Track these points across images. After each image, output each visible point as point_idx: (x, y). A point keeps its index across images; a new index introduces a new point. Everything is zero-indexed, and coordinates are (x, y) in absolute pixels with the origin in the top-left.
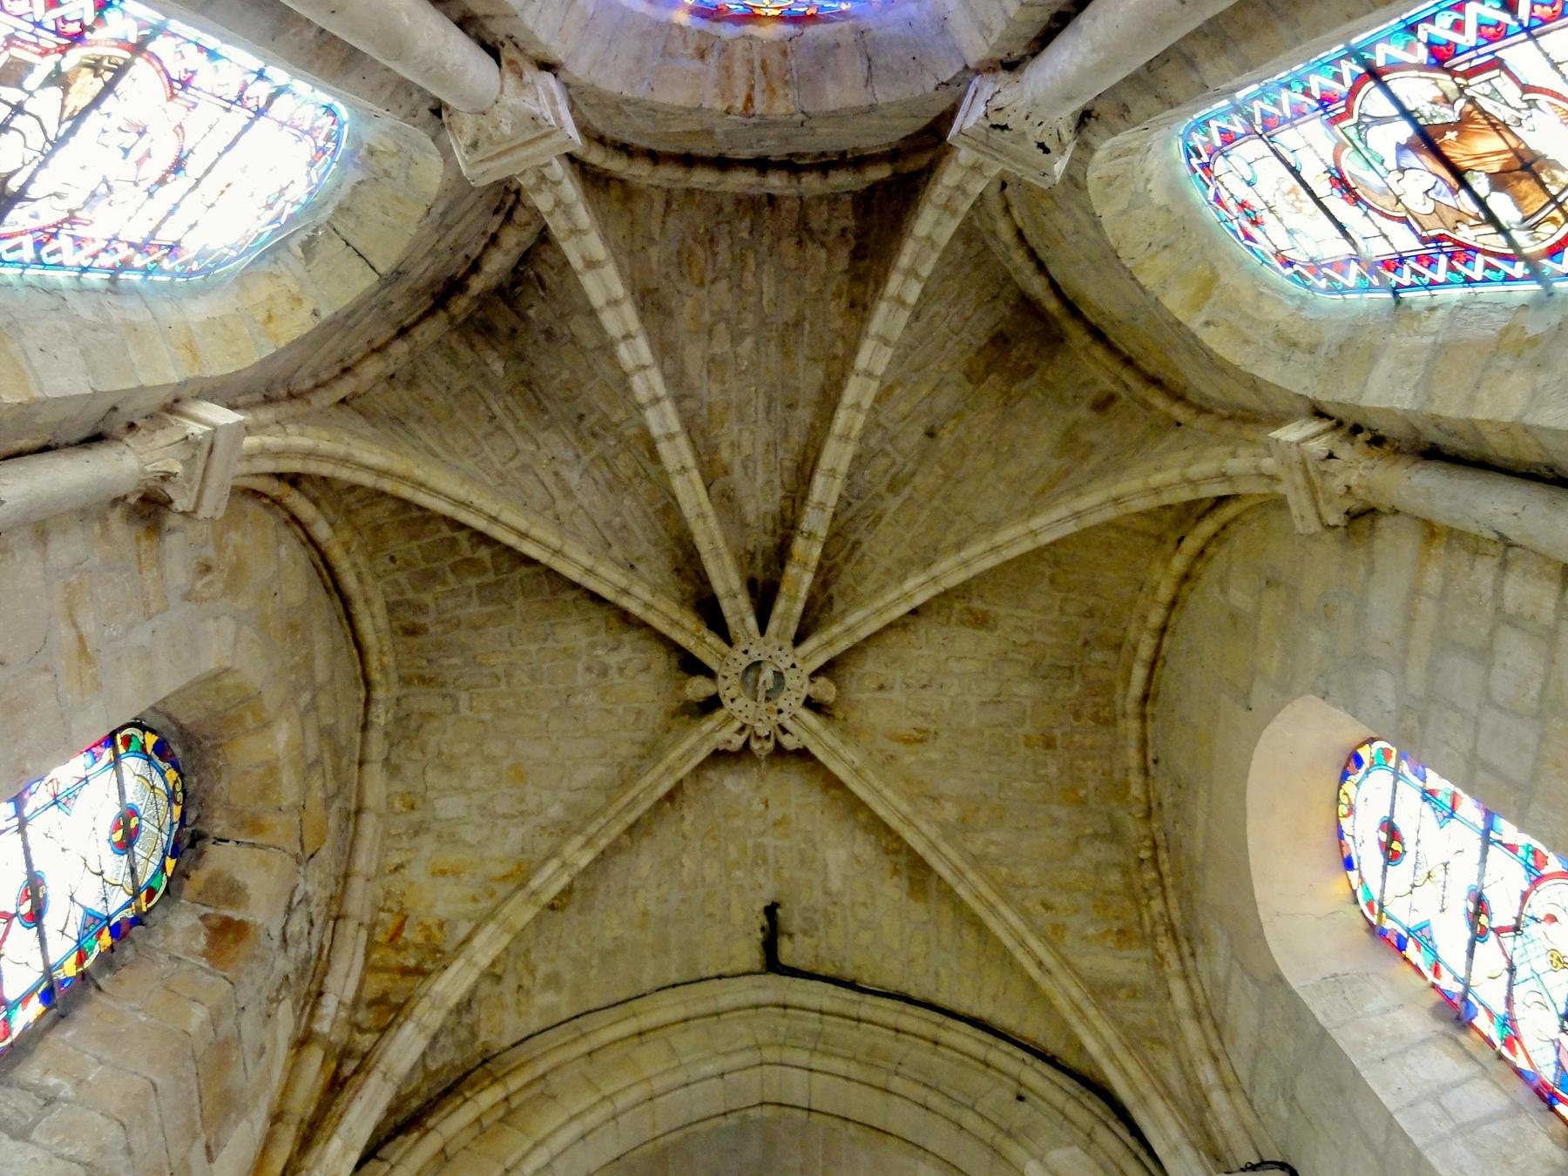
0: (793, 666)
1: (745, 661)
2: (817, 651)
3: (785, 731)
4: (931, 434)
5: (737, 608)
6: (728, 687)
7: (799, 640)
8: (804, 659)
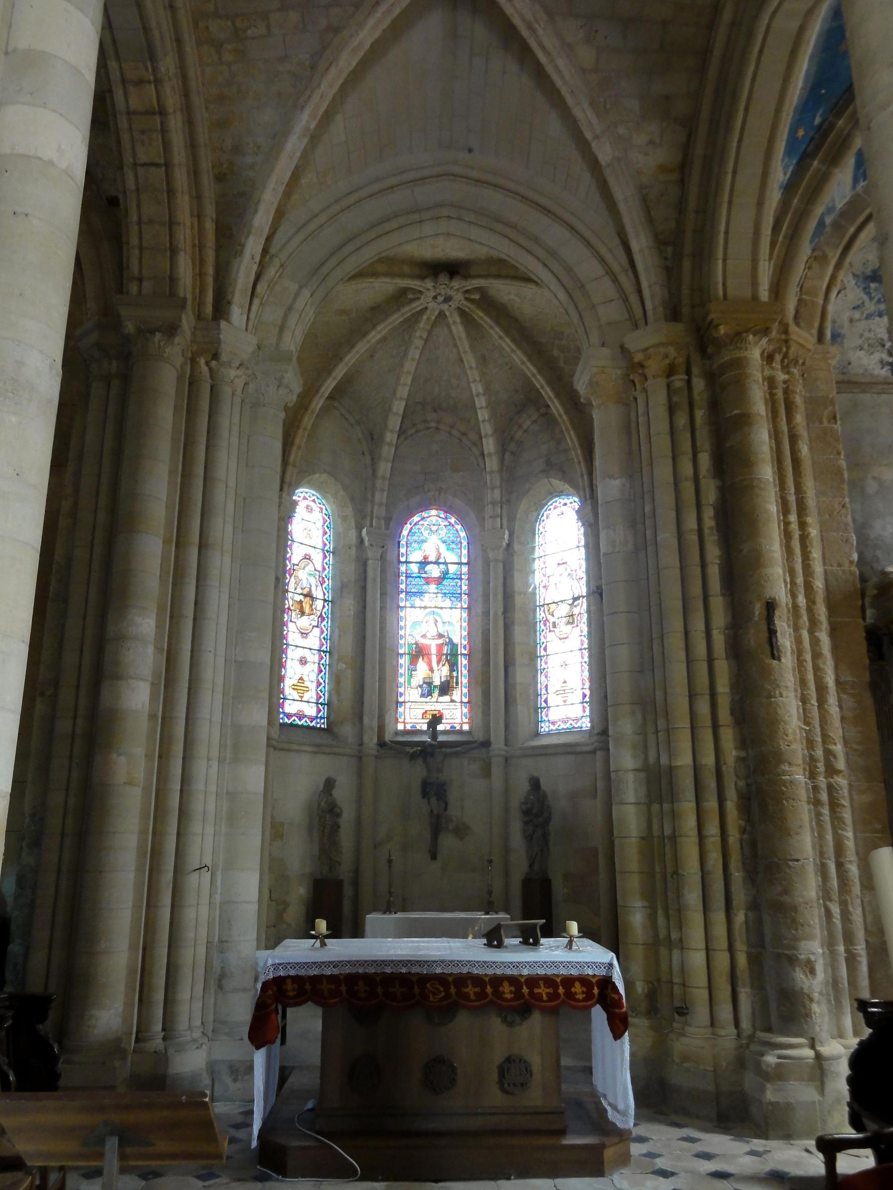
0: (428, 303)
1: (450, 303)
2: (417, 306)
3: (434, 287)
4: (372, 356)
5: (455, 318)
6: (458, 297)
7: (426, 308)
8: (422, 304)
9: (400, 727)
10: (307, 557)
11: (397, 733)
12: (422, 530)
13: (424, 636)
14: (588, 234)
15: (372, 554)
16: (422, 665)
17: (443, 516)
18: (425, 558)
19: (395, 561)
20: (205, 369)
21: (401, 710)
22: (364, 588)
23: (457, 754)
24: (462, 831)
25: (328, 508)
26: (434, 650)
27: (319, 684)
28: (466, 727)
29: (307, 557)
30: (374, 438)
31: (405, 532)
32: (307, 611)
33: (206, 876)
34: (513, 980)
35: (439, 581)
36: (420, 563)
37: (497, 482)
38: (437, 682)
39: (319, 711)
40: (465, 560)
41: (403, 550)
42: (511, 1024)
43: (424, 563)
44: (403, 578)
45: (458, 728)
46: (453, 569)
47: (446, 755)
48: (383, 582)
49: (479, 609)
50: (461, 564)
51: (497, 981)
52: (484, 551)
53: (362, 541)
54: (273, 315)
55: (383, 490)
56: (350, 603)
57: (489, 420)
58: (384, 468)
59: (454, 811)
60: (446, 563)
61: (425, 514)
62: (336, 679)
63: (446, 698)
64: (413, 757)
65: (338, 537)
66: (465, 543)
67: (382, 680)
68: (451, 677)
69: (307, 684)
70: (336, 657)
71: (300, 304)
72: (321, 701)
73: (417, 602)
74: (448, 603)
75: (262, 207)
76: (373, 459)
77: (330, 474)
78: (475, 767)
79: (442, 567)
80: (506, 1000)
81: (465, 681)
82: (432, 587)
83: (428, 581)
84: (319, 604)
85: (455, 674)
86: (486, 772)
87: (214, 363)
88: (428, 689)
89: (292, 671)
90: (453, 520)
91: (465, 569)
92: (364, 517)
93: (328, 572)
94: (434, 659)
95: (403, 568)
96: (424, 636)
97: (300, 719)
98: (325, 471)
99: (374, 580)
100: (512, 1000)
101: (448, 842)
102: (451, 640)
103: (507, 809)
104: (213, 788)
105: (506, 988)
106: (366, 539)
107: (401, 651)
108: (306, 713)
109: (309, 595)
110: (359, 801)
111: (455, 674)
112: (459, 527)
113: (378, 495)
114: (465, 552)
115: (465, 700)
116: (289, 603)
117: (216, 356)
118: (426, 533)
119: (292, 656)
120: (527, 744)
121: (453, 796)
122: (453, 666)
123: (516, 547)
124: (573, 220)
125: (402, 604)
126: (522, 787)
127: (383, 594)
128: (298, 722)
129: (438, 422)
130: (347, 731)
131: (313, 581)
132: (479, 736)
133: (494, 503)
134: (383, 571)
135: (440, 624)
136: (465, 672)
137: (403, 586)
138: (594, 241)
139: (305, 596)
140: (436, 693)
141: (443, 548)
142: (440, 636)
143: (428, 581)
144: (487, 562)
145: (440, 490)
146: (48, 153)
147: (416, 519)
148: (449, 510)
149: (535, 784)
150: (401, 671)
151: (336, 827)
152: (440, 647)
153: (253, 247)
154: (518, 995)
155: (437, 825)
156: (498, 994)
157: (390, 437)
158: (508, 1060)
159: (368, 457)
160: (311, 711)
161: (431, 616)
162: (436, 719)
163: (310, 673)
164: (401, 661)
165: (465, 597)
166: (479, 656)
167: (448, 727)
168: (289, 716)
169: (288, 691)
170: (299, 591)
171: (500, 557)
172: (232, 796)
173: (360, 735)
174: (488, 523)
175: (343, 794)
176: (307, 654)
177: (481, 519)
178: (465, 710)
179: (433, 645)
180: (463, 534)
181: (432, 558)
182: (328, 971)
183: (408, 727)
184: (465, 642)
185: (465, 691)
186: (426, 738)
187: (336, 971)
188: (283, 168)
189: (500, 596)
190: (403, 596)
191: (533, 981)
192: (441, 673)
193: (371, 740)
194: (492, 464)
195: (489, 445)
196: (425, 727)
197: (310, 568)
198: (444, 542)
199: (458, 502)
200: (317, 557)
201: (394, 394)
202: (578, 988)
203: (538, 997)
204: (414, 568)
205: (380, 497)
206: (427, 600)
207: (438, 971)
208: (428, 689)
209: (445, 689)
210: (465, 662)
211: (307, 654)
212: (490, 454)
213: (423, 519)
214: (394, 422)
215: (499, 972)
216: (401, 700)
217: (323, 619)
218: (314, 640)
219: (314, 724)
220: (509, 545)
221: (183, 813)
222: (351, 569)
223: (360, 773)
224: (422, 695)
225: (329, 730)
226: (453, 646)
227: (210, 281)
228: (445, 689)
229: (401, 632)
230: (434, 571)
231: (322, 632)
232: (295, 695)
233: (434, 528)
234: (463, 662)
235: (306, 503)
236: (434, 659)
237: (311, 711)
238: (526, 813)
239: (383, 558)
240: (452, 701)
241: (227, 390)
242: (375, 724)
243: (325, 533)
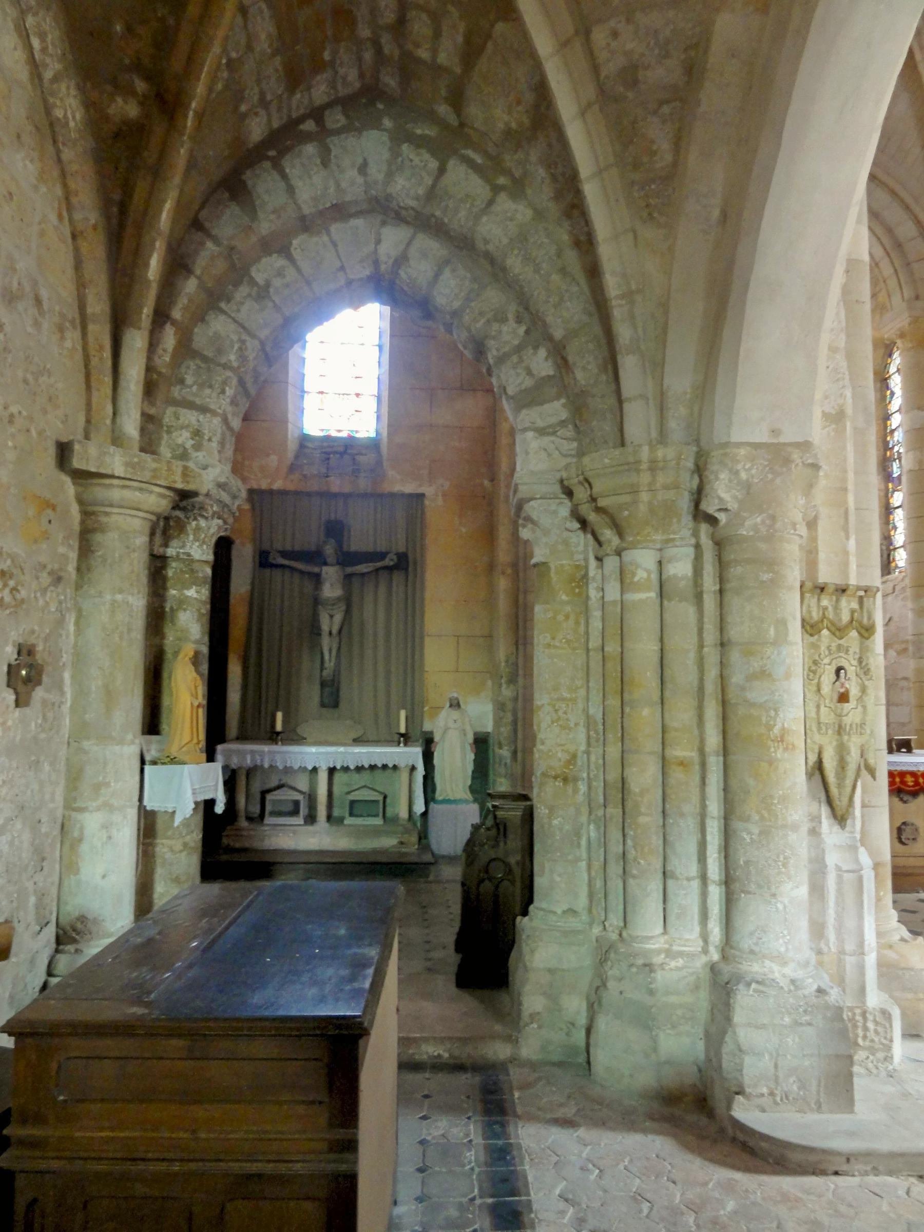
14: (909, 200)
34: (913, 774)
80: (909, 786)
100: (913, 786)
105: (910, 780)
124: (898, 188)
138: (913, 206)
154: (917, 783)
156: (903, 782)
158: (904, 823)
215: (905, 768)
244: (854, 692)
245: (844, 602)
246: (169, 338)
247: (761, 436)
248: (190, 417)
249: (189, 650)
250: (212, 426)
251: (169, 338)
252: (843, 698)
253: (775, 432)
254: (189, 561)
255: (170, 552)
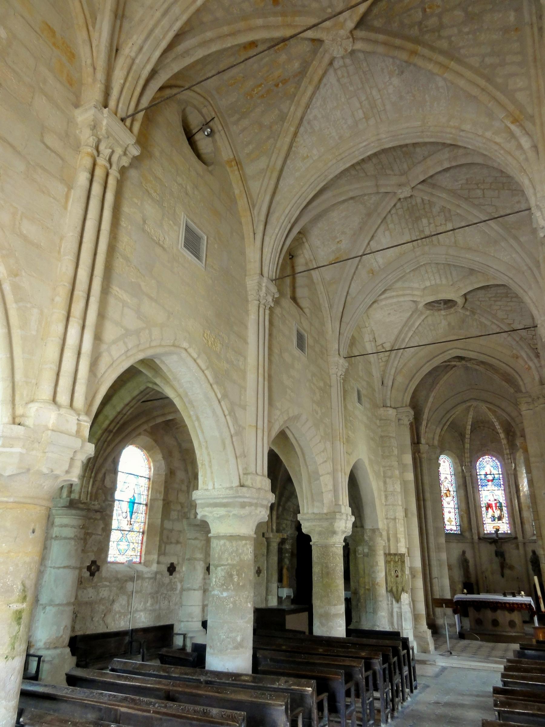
9: (486, 532)
10: (446, 478)
11: (485, 534)
12: (484, 463)
13: (490, 500)
15: (468, 475)
16: (490, 510)
17: (490, 457)
18: (486, 473)
19: (476, 475)
20: (417, 455)
21: (485, 526)
22: (466, 486)
23: (506, 542)
24: (511, 568)
25: (450, 460)
26: (494, 505)
27: (456, 519)
28: (509, 532)
29: (446, 478)
30: (462, 436)
31: (478, 464)
32: (448, 496)
33: (436, 579)
34: (509, 603)
35: (492, 480)
36: (485, 475)
37: (507, 447)
38: (496, 516)
39: (457, 528)
40: (500, 473)
41: (478, 471)
42: (510, 613)
43: (486, 475)
44: (479, 480)
45: (506, 532)
46: (497, 476)
47: (502, 542)
48: (472, 483)
49: (507, 491)
50: (499, 474)
51: (505, 603)
52: (507, 470)
53: (463, 470)
54: (431, 436)
55: (467, 453)
56: (462, 492)
57: (500, 429)
58: (467, 446)
59: (508, 561)
60: (493, 474)
61: (484, 458)
62: (461, 517)
63: (500, 522)
64: (491, 543)
65: (455, 469)
66: (500, 467)
67: (477, 516)
68: (501, 514)
69: (452, 519)
70: (460, 509)
71: (437, 432)
72: (457, 524)
73: (485, 488)
74: (496, 488)
75: (425, 414)
76: (463, 442)
77: (449, 450)
78: (513, 546)
79: (493, 476)
81: (507, 515)
82: (490, 483)
83: (488, 481)
84: (452, 493)
85: (502, 513)
86: (517, 547)
87: (419, 454)
88: (493, 518)
89: (447, 516)
90: (494, 459)
91: (501, 476)
92: (463, 462)
93: (453, 481)
94: (494, 508)
95: (479, 477)
96: (490, 500)
97: (451, 531)
98: (448, 450)
99: (469, 483)
101: (507, 572)
102: (499, 501)
103: (526, 560)
104: (435, 559)
106: (464, 470)
107: (482, 506)
108: (453, 529)
109: (448, 490)
110: (474, 557)
111: (502, 513)
112: (497, 461)
113: (466, 454)
114: (500, 470)
115: (508, 522)
116: (442, 494)
117: (419, 452)
118: (485, 464)
119: (446, 511)
120: (530, 539)
121: (507, 556)
122: (501, 510)
123: (518, 469)
125: (480, 490)
126: (530, 554)
127: (473, 487)
128: (451, 532)
129: (484, 427)
130: (467, 534)
131: (449, 485)
132: (514, 536)
133: (507, 454)
134: (472, 479)
135: (494, 495)
136: (506, 512)
137: (479, 483)
139: (447, 491)
140: (497, 520)
141: (492, 469)
142: (495, 500)
143: (488, 481)
144: (508, 474)
145: (488, 450)
146: (410, 479)
147: (481, 459)
148: (493, 456)
149: (534, 552)
150: (483, 513)
151: (468, 567)
152: (496, 504)
153: (424, 423)
154: (510, 606)
155: (503, 566)
157: (468, 436)
159: (461, 442)
160: (454, 528)
161: (491, 493)
162: (498, 530)
163: (452, 516)
164: (483, 509)
165: (502, 486)
166: (510, 507)
167: (503, 532)
168: (448, 530)
169: (446, 523)
170: (445, 489)
171: (512, 473)
172: (439, 560)
173: (472, 536)
174: (506, 461)
175: (469, 555)
176: (450, 509)
177: (504, 459)
178: (508, 526)
179: (493, 503)
180: (499, 464)
181: (488, 473)
182: (468, 600)
183: (488, 532)
184: (505, 502)
185: (507, 519)
186: (494, 536)
187: (470, 600)
188: (429, 404)
189: (514, 486)
190: (480, 486)
191: (513, 604)
192: (497, 513)
193: (476, 537)
194: (504, 442)
195: (502, 436)
196: (494, 532)
197: (447, 481)
198: (492, 467)
199: (494, 453)
200: (449, 477)
201: (467, 423)
202: (524, 606)
203: (515, 607)
204: (483, 477)
205: (467, 455)
206: (489, 487)
207: (491, 601)
208: (493, 518)
209: (500, 518)
210: (506, 509)
211: (450, 509)
212: (503, 439)
213: (483, 459)
214: (468, 432)
216: (484, 522)
217: (454, 497)
218: (452, 505)
219: (456, 532)
220: (515, 468)
221: (429, 565)
222: (461, 481)
223: (473, 548)
224: (492, 521)
225: (461, 534)
226: (501, 503)
227: (415, 434)
228: (500, 518)
229: (481, 499)
230: (490, 477)
231: (454, 502)
232: (448, 523)
233: (488, 462)
234: (505, 509)
235: (443, 460)
236: (494, 508)
237: (454, 528)
238: (532, 562)
239: (471, 476)
240: (503, 523)
241: (423, 460)
242: (476, 532)
243: (450, 469)
244: (400, 575)
245: (396, 557)
246: (281, 509)
247: (370, 527)
248: (285, 522)
249: (286, 566)
250: (289, 523)
251: (281, 509)
252: (397, 576)
253: (373, 527)
254: (286, 549)
255: (283, 547)
